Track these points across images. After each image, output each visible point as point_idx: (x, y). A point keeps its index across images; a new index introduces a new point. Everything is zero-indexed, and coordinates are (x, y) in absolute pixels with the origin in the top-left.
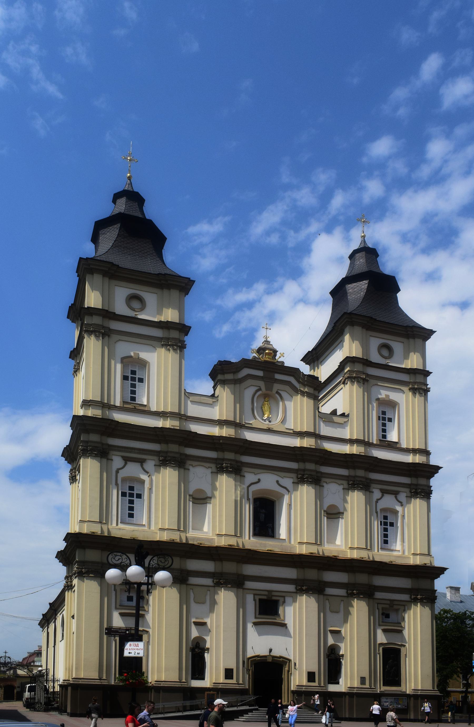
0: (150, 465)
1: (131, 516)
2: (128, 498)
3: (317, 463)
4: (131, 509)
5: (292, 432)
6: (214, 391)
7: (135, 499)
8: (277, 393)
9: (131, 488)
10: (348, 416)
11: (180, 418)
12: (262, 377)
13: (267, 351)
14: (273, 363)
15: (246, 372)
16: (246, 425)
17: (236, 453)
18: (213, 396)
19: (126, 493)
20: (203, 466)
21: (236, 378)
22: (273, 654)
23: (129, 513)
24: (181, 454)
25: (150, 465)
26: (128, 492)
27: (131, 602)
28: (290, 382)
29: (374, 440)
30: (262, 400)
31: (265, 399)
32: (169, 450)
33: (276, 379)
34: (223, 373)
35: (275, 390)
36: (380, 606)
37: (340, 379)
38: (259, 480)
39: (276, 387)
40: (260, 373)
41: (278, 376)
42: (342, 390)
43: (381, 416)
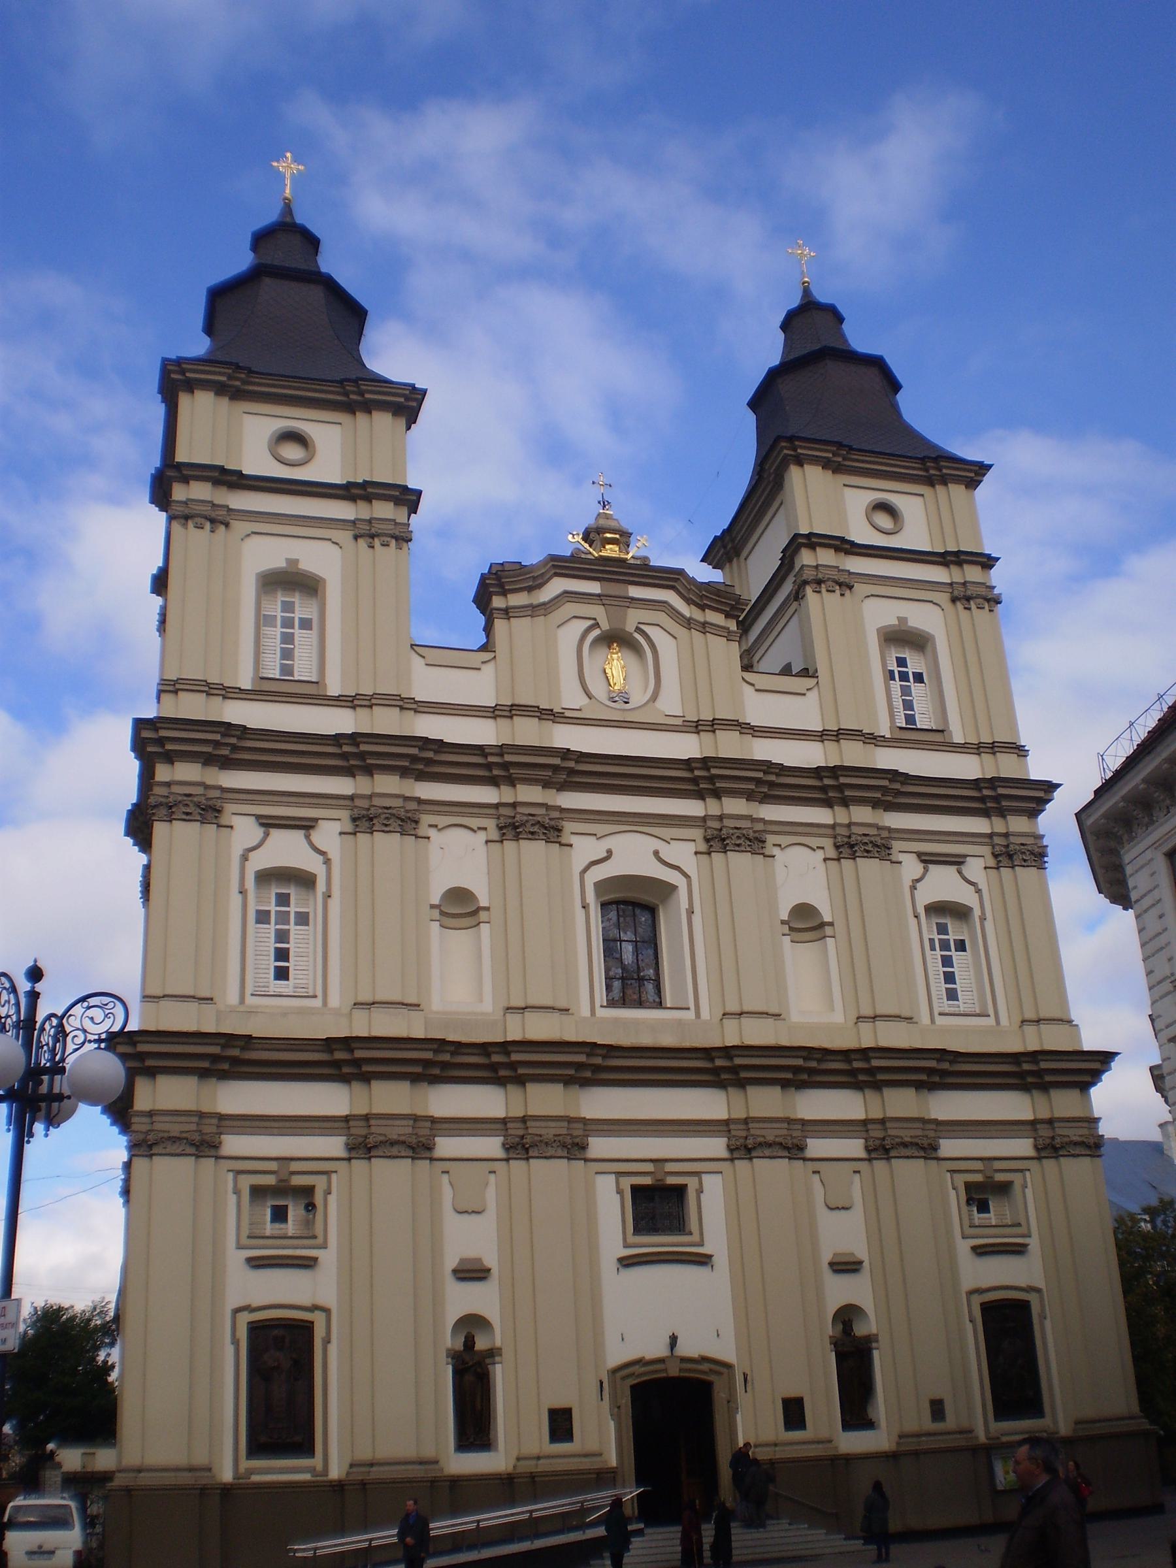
0: (329, 834)
1: (282, 974)
2: (272, 927)
3: (750, 796)
4: (282, 955)
5: (679, 722)
6: (488, 636)
7: (292, 927)
8: (638, 630)
9: (283, 900)
10: (814, 676)
11: (402, 708)
12: (599, 595)
13: (608, 535)
14: (624, 561)
15: (557, 586)
16: (568, 714)
17: (546, 785)
18: (484, 648)
19: (269, 912)
20: (461, 826)
21: (535, 602)
22: (684, 1349)
23: (276, 967)
24: (407, 799)
25: (329, 834)
26: (273, 908)
27: (282, 1226)
28: (665, 602)
29: (885, 731)
30: (602, 651)
31: (609, 647)
32: (377, 790)
33: (633, 599)
34: (504, 593)
35: (630, 627)
36: (961, 1179)
37: (787, 588)
38: (610, 853)
39: (633, 618)
40: (594, 587)
41: (635, 592)
42: (795, 618)
43: (896, 670)
